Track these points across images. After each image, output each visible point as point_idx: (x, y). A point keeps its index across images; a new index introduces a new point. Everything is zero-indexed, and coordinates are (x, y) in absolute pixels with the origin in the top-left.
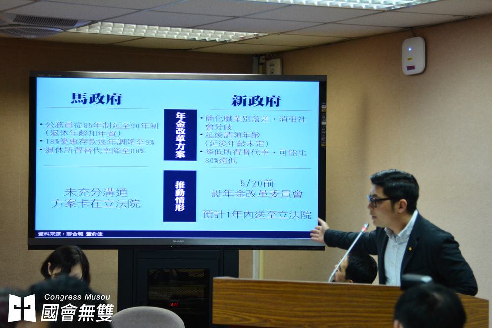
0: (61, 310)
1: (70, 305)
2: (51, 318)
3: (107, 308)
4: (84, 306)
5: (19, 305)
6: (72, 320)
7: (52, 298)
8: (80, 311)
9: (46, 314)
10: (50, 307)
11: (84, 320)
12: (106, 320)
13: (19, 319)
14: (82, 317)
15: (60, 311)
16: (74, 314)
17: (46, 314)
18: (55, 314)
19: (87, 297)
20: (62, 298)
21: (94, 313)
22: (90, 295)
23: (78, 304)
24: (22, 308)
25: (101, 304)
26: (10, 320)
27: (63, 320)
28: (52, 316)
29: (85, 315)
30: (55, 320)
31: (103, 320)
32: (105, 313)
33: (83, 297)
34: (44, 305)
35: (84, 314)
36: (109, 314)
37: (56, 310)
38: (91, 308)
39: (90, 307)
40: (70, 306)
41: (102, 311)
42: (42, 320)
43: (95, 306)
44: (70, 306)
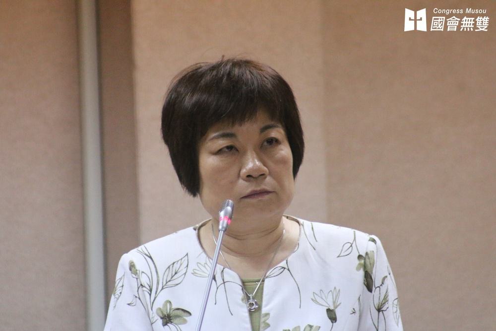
0: (447, 21)
1: (454, 17)
2: (439, 28)
3: (484, 20)
4: (465, 18)
5: (413, 18)
6: (455, 30)
7: (440, 11)
8: (462, 22)
9: (434, 25)
10: (438, 19)
11: (465, 30)
12: (483, 29)
13: (412, 28)
14: (464, 28)
15: (446, 22)
16: (457, 24)
17: (434, 25)
18: (442, 25)
19: (468, 11)
20: (448, 11)
21: (473, 24)
22: (470, 9)
23: (461, 16)
24: (415, 20)
25: (479, 17)
26: (406, 29)
27: (448, 30)
28: (439, 27)
29: (466, 26)
30: (442, 30)
31: (481, 29)
32: (482, 24)
33: (464, 11)
34: (433, 18)
35: (465, 25)
36: (486, 25)
37: (442, 22)
38: (471, 21)
39: (470, 19)
40: (454, 19)
41: (480, 23)
42: (432, 30)
43: (474, 18)
44: (454, 19)
